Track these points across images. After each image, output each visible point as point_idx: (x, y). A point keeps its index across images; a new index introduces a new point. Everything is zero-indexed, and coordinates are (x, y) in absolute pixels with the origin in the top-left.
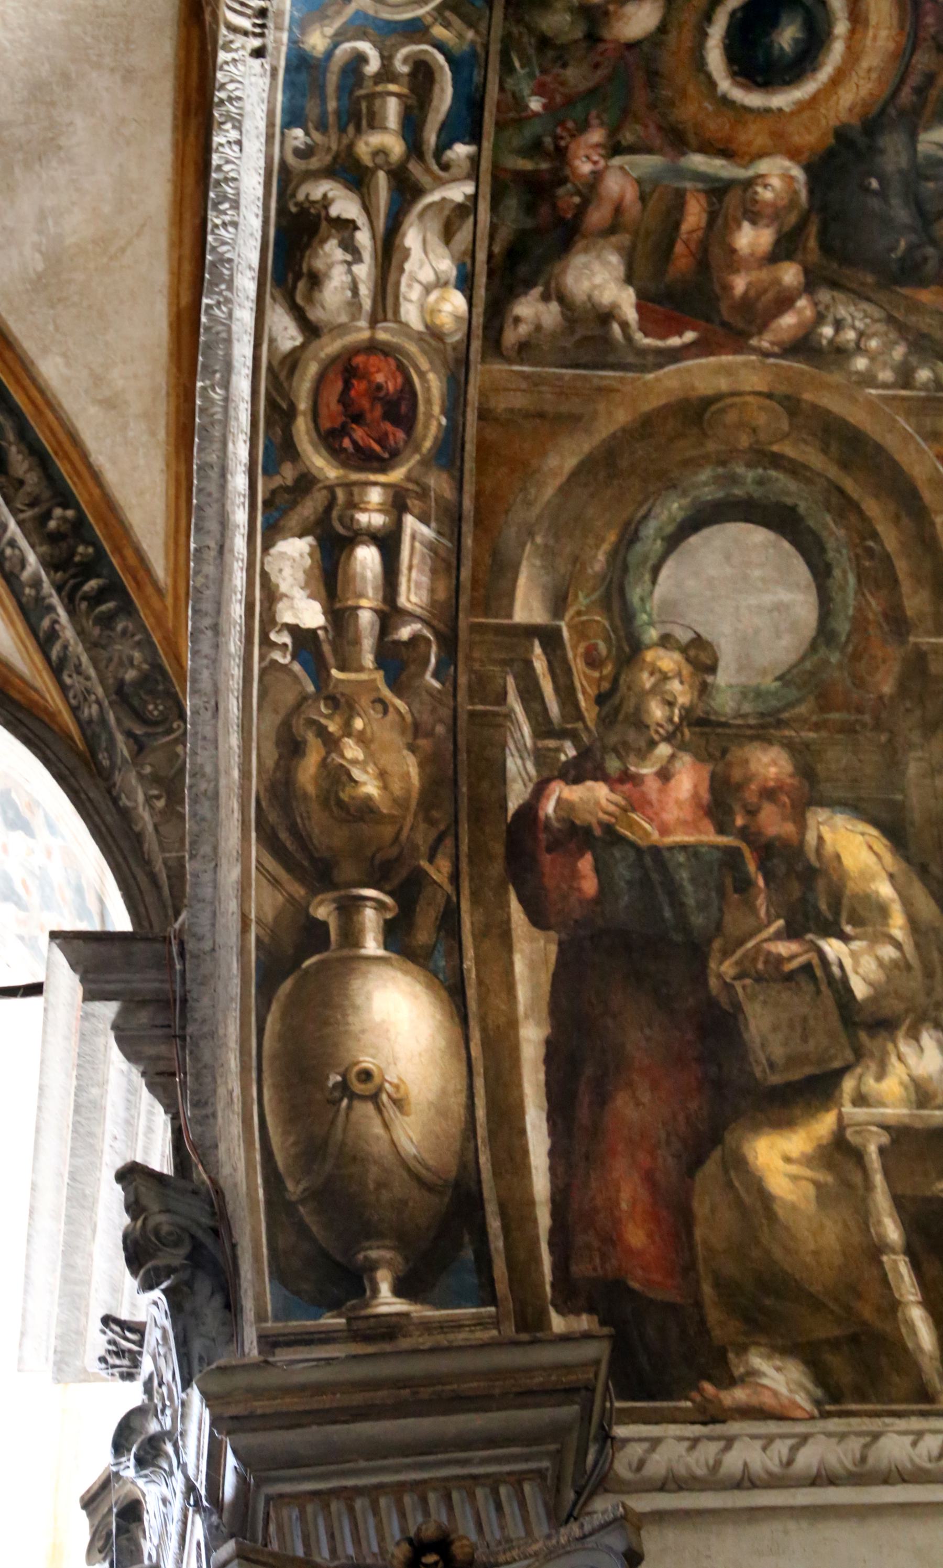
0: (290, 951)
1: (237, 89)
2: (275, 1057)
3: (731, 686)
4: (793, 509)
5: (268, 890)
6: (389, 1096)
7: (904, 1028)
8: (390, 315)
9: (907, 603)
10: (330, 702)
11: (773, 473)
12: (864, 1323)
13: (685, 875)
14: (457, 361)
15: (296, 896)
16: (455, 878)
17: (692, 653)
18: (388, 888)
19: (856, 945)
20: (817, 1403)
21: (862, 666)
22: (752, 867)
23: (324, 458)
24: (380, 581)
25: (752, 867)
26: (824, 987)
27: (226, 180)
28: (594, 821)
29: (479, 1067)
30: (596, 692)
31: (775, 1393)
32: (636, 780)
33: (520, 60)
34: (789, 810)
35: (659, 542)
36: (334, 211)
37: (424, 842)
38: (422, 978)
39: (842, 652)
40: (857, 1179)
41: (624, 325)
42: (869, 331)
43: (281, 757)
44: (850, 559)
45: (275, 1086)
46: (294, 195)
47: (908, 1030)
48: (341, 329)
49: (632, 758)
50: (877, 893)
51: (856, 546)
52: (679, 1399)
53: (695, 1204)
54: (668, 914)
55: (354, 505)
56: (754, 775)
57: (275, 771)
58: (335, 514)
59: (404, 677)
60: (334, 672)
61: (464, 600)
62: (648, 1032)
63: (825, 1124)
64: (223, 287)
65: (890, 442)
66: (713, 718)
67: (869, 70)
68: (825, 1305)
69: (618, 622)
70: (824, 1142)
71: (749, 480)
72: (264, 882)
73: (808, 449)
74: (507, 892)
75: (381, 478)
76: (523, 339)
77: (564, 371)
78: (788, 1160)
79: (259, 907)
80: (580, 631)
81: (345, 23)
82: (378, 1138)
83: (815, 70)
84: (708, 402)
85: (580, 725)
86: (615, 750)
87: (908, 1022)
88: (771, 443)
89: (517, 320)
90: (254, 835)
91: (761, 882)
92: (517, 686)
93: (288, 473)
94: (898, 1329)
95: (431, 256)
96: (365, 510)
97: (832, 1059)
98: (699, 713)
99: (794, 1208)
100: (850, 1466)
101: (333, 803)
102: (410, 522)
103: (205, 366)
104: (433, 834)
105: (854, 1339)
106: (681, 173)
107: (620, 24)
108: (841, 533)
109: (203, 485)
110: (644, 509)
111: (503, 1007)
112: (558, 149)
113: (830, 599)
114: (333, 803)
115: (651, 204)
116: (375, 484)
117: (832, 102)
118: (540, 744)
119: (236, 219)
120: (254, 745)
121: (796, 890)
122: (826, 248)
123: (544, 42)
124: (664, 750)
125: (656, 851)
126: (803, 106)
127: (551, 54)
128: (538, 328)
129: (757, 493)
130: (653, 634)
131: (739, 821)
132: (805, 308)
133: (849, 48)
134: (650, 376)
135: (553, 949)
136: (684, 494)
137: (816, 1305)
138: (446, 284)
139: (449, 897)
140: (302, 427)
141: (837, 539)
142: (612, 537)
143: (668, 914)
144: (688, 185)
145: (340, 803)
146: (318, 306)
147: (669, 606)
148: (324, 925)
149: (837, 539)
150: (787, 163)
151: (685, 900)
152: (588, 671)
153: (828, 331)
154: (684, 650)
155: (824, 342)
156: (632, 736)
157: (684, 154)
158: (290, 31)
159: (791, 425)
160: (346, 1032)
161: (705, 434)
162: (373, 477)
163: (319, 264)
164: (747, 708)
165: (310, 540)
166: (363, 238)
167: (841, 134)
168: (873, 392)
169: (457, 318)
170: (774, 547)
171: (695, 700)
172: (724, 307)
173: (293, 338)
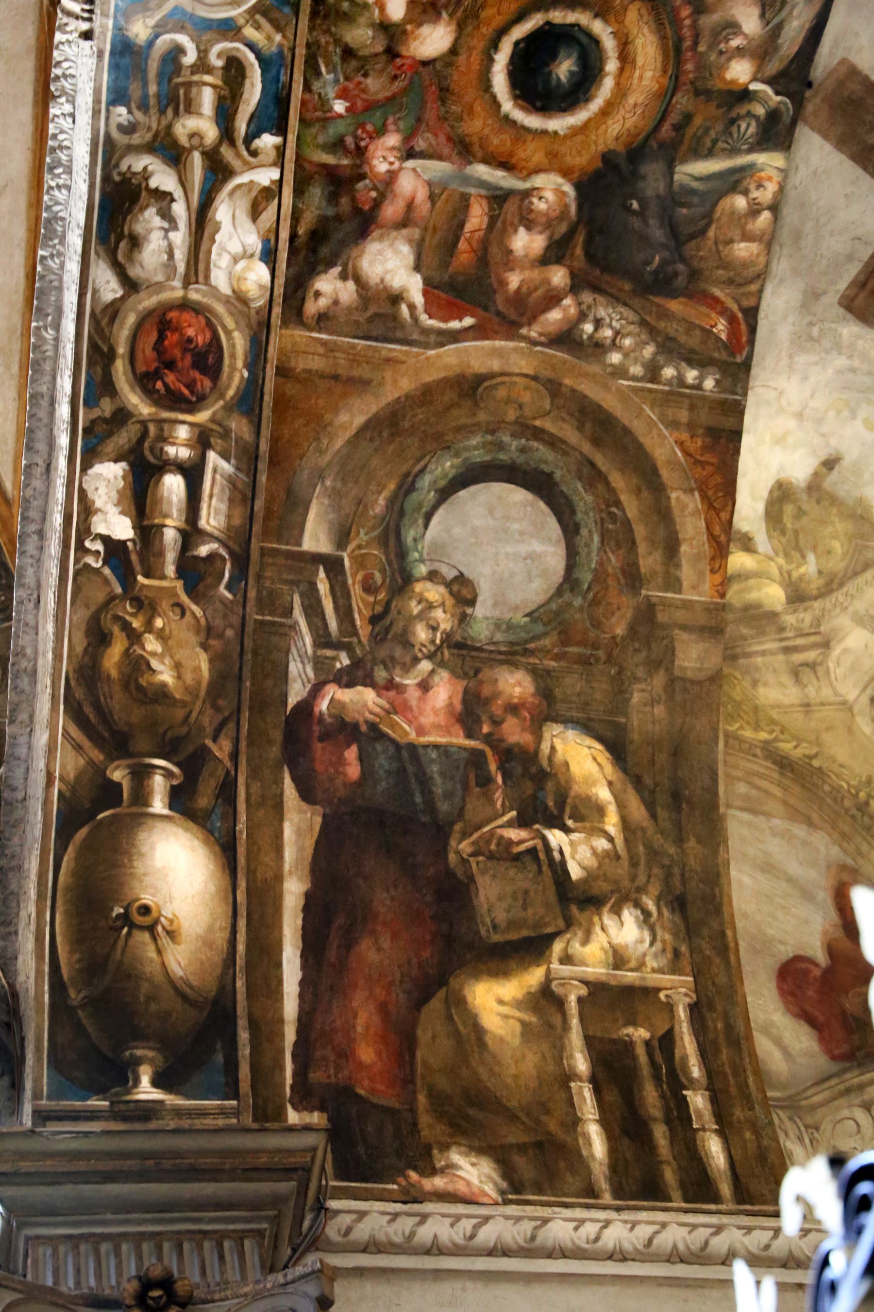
0: (87, 805)
1: (70, 67)
2: (68, 889)
3: (486, 618)
4: (550, 475)
5: (71, 754)
6: (164, 928)
7: (609, 905)
8: (201, 278)
9: (641, 562)
10: (134, 603)
11: (535, 444)
12: (549, 1133)
13: (435, 768)
14: (259, 323)
15: (96, 761)
16: (235, 756)
17: (455, 588)
18: (176, 760)
19: (575, 836)
20: (502, 1193)
21: (600, 611)
22: (493, 767)
23: (140, 397)
24: (184, 505)
25: (493, 767)
26: (545, 868)
27: (61, 148)
28: (361, 719)
29: (243, 911)
30: (371, 614)
31: (468, 1183)
32: (400, 689)
33: (327, 66)
34: (528, 723)
35: (432, 493)
36: (153, 183)
37: (210, 724)
38: (200, 835)
39: (584, 598)
40: (557, 1020)
41: (412, 307)
42: (624, 331)
43: (89, 645)
44: (596, 522)
45: (67, 914)
46: (117, 165)
47: (612, 907)
48: (159, 287)
49: (398, 670)
50: (597, 795)
51: (601, 511)
52: (388, 1183)
53: (419, 1032)
54: (418, 799)
55: (164, 438)
56: (500, 693)
57: (83, 657)
58: (146, 445)
59: (201, 587)
60: (140, 578)
61: (257, 528)
62: (393, 892)
63: (535, 977)
64: (56, 241)
65: (637, 427)
66: (469, 642)
67: (635, 105)
68: (518, 1118)
69: (392, 556)
70: (533, 990)
71: (513, 448)
72: (69, 747)
73: (565, 426)
74: (282, 771)
75: (189, 418)
76: (322, 311)
77: (356, 341)
78: (501, 1002)
79: (63, 766)
80: (360, 562)
81: (165, 16)
82: (152, 961)
83: (587, 100)
84: (481, 379)
85: (355, 640)
86: (383, 662)
87: (612, 900)
88: (534, 418)
89: (317, 294)
90: (62, 707)
91: (500, 780)
92: (302, 603)
93: (106, 407)
94: (577, 1140)
95: (239, 230)
96: (173, 444)
97: (546, 925)
98: (458, 637)
99: (502, 1040)
100: (522, 1243)
101: (132, 686)
102: (212, 457)
103: (39, 309)
104: (218, 718)
105: (539, 1145)
106: (467, 180)
107: (417, 43)
108: (589, 499)
109: (34, 411)
110: (422, 463)
111: (271, 864)
112: (358, 147)
113: (577, 553)
114: (132, 686)
115: (438, 205)
116: (183, 422)
117: (601, 131)
118: (319, 653)
119: (68, 182)
120: (67, 633)
121: (529, 788)
122: (589, 256)
123: (348, 53)
124: (425, 666)
125: (412, 747)
126: (576, 131)
127: (354, 63)
128: (336, 302)
129: (520, 459)
130: (422, 570)
131: (486, 729)
132: (569, 306)
133: (618, 84)
134: (432, 352)
135: (319, 820)
136: (457, 455)
137: (512, 1116)
138: (252, 256)
139: (228, 772)
140: (120, 368)
141: (585, 503)
142: (392, 486)
143: (418, 799)
144: (473, 191)
145: (139, 688)
146: (137, 265)
147: (436, 546)
148: (119, 786)
149: (585, 503)
150: (560, 180)
151: (434, 789)
152: (363, 594)
153: (588, 328)
154: (448, 585)
155: (585, 337)
156: (398, 652)
157: (470, 163)
159: (552, 404)
160: (132, 874)
161: (476, 404)
162: (181, 417)
163: (139, 229)
164: (499, 637)
165: (123, 465)
166: (179, 209)
167: (608, 158)
168: (625, 383)
169: (261, 287)
170: (532, 506)
171: (455, 628)
172: (499, 299)
173: (113, 290)
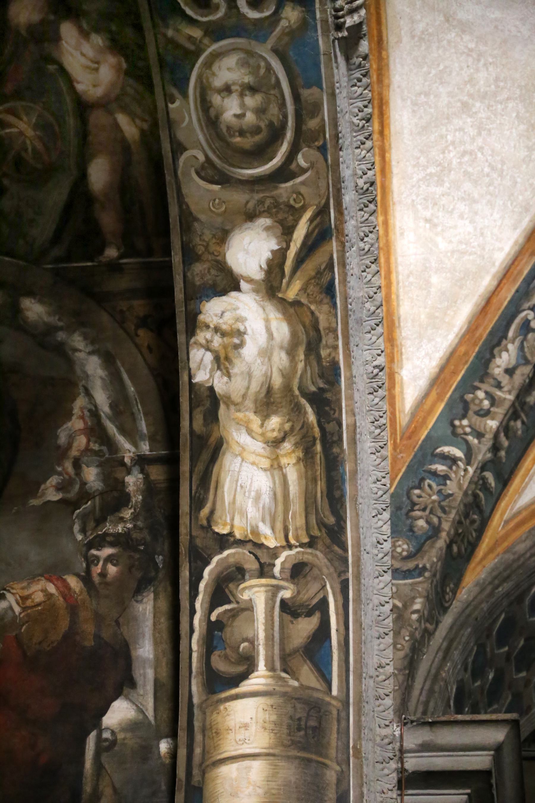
158: (315, 18)
